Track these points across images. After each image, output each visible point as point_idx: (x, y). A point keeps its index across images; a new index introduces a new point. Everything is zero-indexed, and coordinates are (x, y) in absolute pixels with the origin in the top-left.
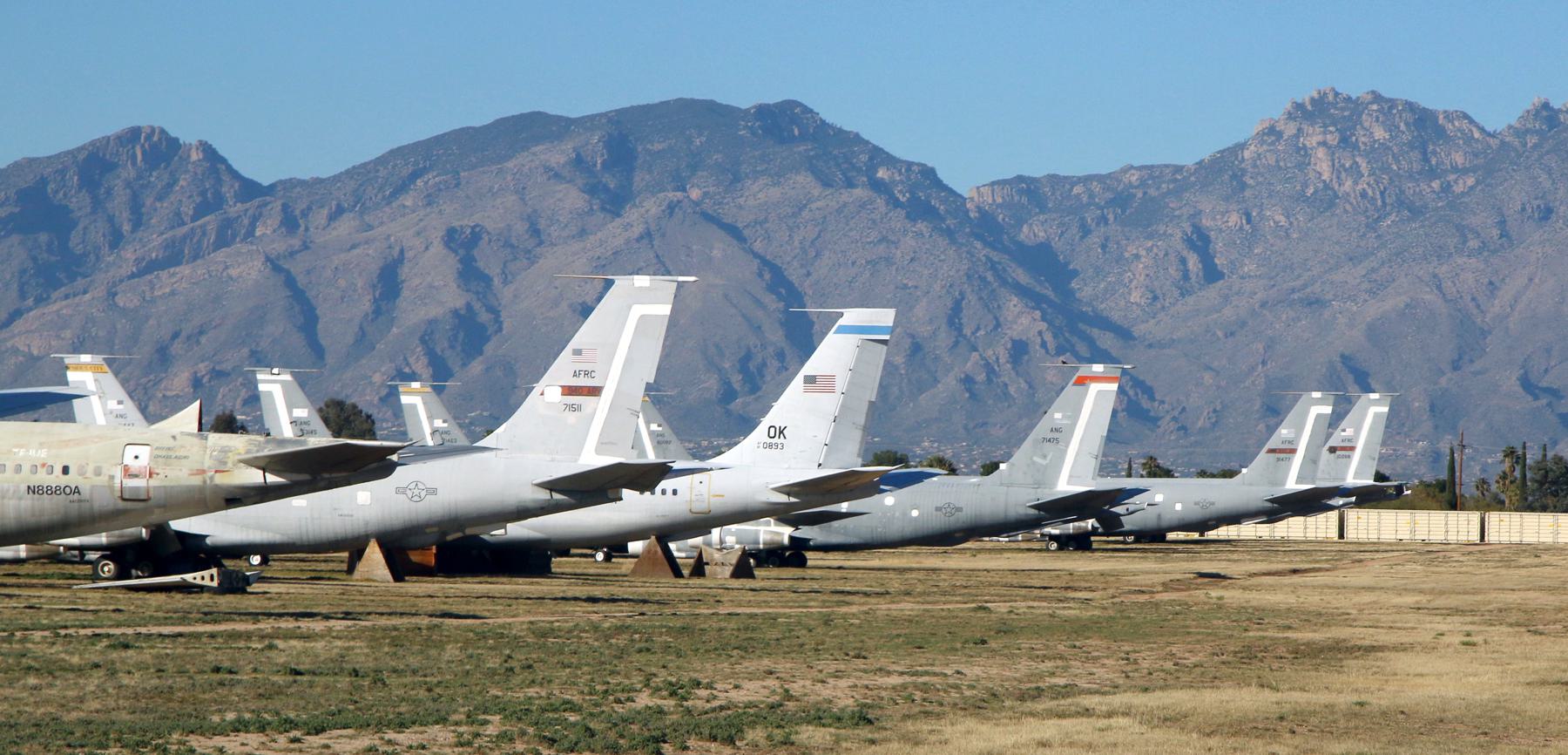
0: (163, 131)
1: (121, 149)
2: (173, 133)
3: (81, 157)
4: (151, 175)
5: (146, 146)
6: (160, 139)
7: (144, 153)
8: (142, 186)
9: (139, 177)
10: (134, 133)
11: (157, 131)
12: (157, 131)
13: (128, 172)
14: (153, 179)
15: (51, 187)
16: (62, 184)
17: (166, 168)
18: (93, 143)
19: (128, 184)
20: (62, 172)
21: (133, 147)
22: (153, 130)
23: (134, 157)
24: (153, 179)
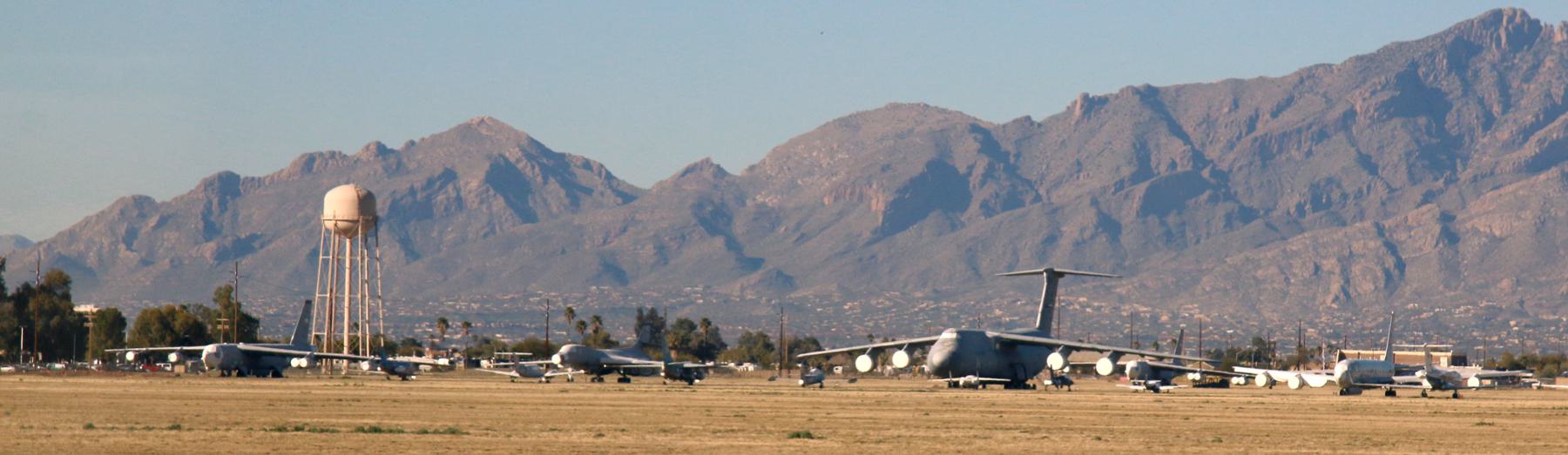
0: (1524, 14)
1: (1484, 32)
2: (1533, 16)
3: (1449, 40)
4: (1515, 57)
5: (1510, 28)
6: (1523, 21)
7: (1508, 35)
8: (1507, 68)
9: (1503, 59)
10: (1497, 15)
11: (1519, 13)
12: (1519, 13)
13: (1492, 54)
14: (1516, 61)
15: (1422, 70)
16: (1432, 67)
17: (1528, 50)
18: (1458, 27)
19: (1494, 66)
20: (1432, 55)
21: (1497, 30)
22: (1515, 12)
23: (1499, 39)
24: (1516, 61)
